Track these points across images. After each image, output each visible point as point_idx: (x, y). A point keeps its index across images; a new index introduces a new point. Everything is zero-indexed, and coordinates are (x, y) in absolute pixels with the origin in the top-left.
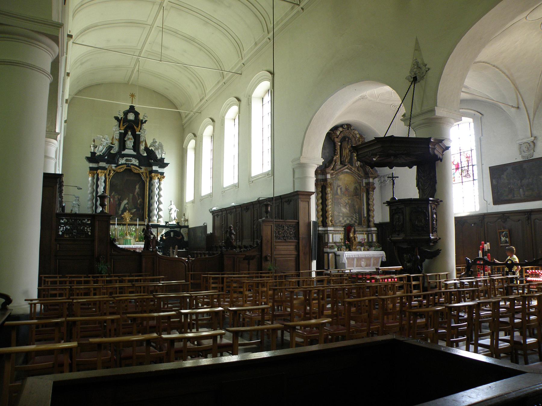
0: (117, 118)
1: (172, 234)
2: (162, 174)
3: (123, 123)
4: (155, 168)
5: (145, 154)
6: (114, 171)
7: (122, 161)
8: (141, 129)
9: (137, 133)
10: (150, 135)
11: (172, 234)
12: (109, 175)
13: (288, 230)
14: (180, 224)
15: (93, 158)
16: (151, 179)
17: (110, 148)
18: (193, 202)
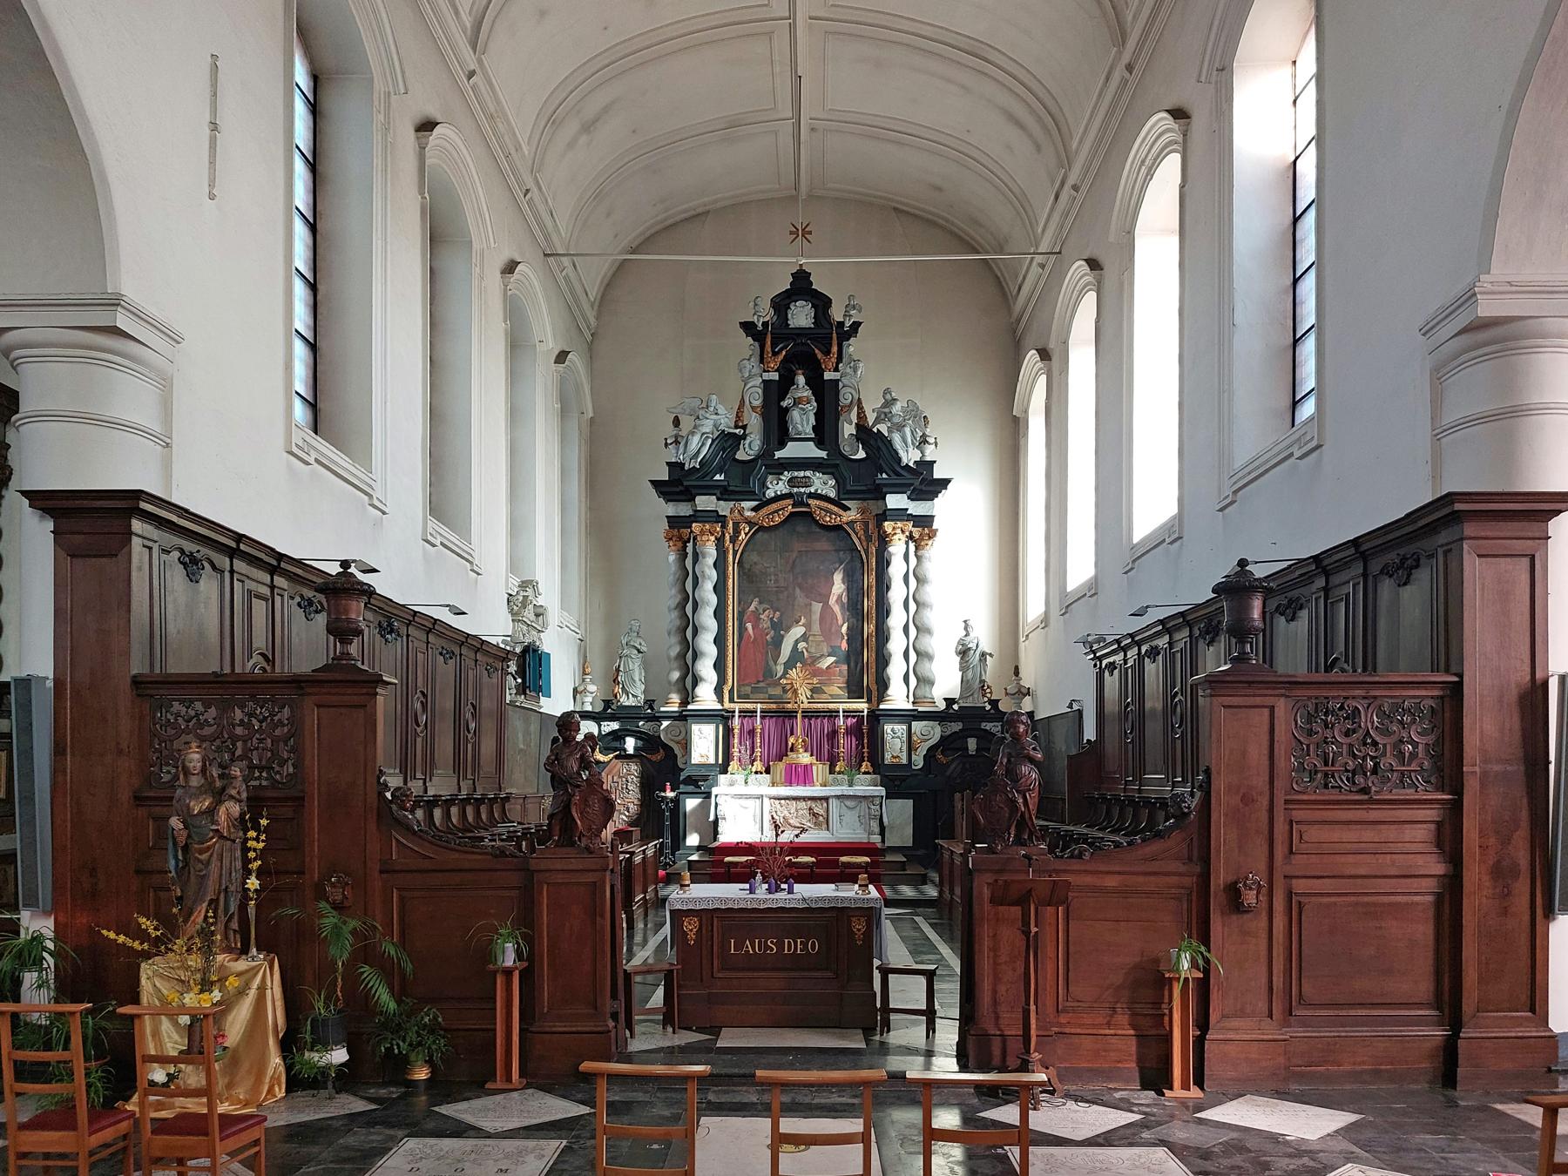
0: (748, 327)
1: (972, 744)
2: (925, 522)
3: (774, 345)
4: (894, 501)
5: (861, 454)
6: (750, 523)
7: (777, 486)
8: (840, 359)
9: (828, 376)
10: (871, 378)
11: (972, 744)
12: (734, 540)
13: (1385, 732)
14: (1002, 707)
15: (678, 484)
16: (884, 541)
17: (729, 441)
18: (1045, 621)
